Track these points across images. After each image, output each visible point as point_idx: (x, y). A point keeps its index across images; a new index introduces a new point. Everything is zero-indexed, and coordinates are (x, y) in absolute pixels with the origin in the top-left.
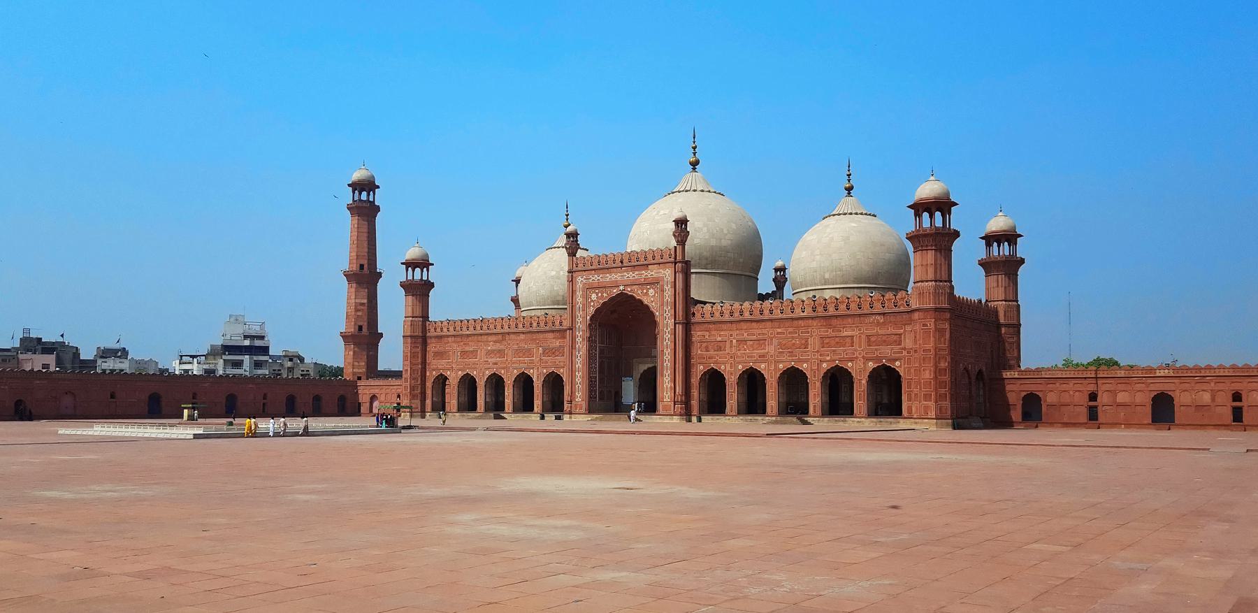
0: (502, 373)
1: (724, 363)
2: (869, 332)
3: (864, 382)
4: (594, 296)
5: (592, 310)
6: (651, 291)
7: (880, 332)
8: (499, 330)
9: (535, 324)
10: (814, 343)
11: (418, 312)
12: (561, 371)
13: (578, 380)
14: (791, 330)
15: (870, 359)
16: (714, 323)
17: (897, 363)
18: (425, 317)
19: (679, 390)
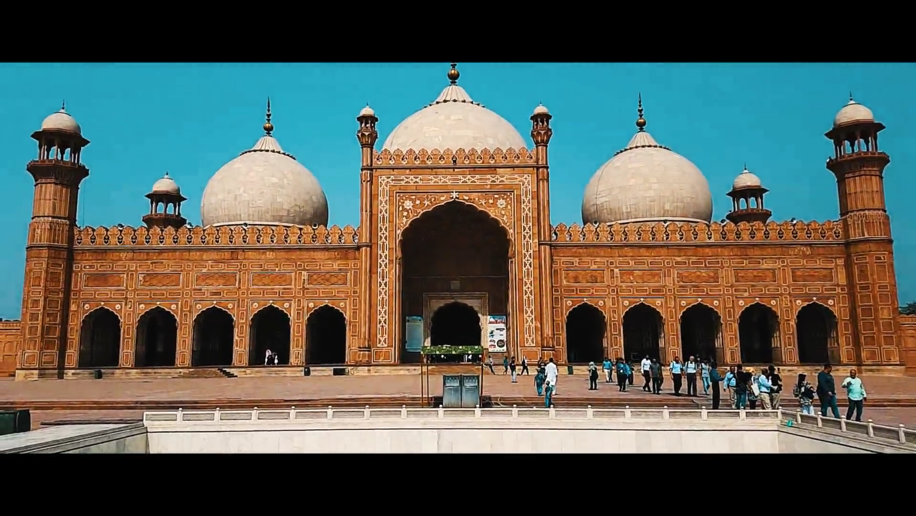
0: (230, 307)
1: (601, 298)
2: (794, 266)
3: (793, 323)
4: (408, 204)
5: (405, 222)
6: (501, 203)
7: (811, 265)
8: (224, 242)
9: (293, 239)
10: (727, 276)
11: (63, 211)
12: (340, 306)
13: (382, 317)
14: (694, 259)
15: (797, 297)
16: (586, 247)
17: (831, 302)
18: (72, 217)
19: (548, 331)
